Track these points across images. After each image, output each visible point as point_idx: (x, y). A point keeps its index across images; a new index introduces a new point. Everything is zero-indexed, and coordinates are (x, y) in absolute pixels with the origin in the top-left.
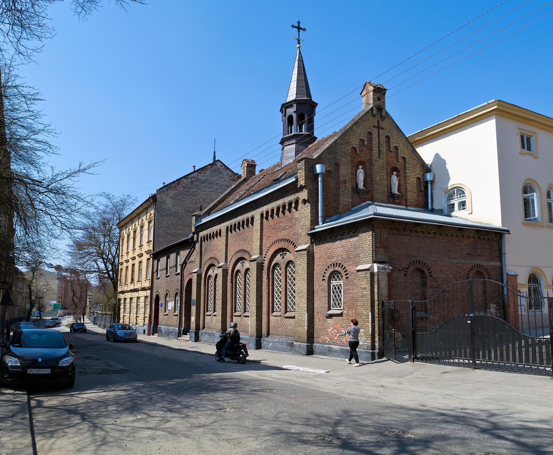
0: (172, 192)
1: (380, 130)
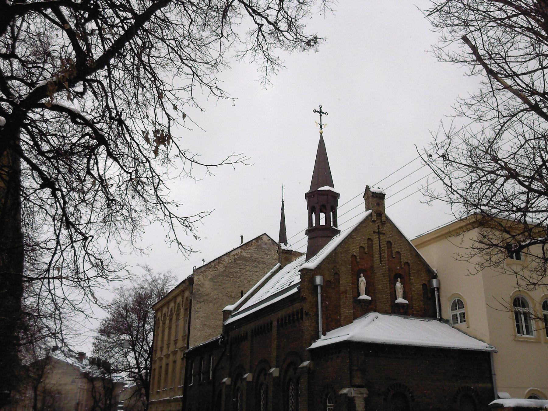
0: (212, 273)
1: (381, 236)
